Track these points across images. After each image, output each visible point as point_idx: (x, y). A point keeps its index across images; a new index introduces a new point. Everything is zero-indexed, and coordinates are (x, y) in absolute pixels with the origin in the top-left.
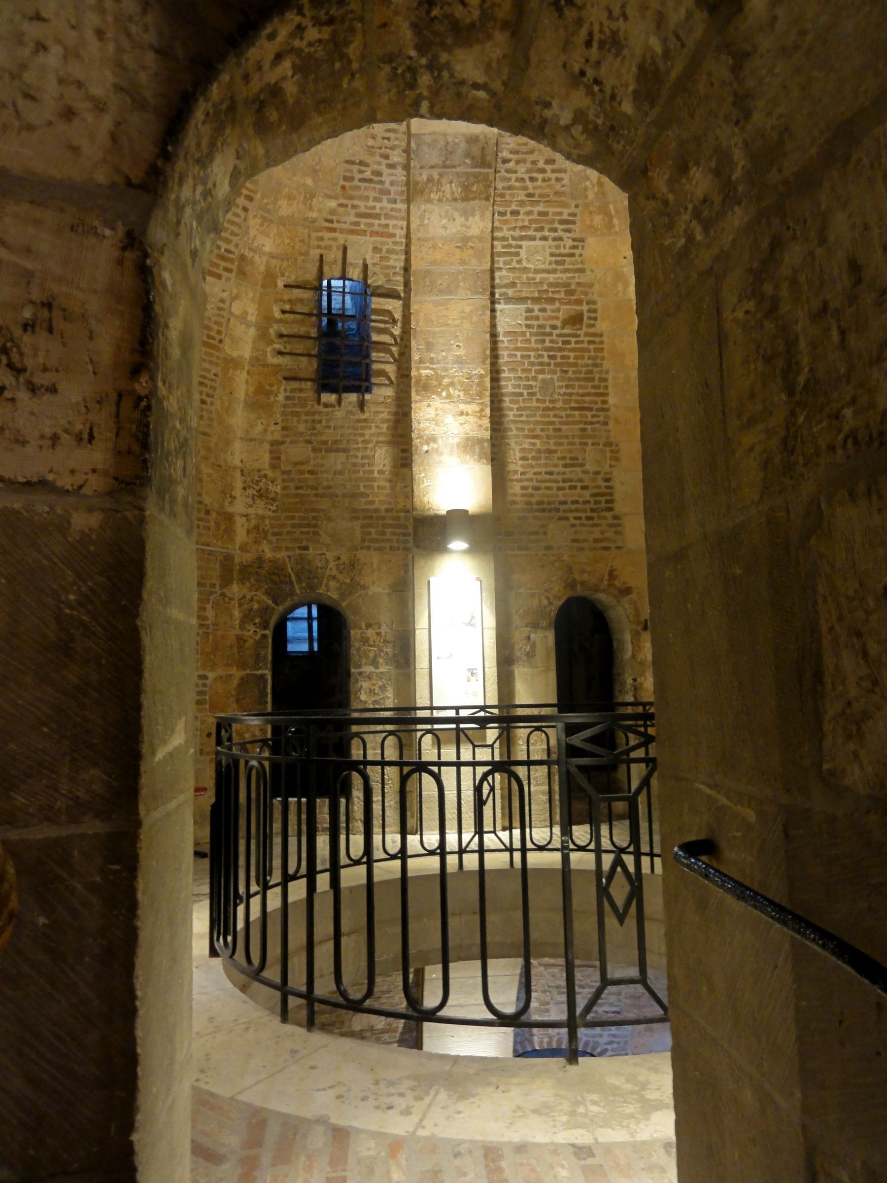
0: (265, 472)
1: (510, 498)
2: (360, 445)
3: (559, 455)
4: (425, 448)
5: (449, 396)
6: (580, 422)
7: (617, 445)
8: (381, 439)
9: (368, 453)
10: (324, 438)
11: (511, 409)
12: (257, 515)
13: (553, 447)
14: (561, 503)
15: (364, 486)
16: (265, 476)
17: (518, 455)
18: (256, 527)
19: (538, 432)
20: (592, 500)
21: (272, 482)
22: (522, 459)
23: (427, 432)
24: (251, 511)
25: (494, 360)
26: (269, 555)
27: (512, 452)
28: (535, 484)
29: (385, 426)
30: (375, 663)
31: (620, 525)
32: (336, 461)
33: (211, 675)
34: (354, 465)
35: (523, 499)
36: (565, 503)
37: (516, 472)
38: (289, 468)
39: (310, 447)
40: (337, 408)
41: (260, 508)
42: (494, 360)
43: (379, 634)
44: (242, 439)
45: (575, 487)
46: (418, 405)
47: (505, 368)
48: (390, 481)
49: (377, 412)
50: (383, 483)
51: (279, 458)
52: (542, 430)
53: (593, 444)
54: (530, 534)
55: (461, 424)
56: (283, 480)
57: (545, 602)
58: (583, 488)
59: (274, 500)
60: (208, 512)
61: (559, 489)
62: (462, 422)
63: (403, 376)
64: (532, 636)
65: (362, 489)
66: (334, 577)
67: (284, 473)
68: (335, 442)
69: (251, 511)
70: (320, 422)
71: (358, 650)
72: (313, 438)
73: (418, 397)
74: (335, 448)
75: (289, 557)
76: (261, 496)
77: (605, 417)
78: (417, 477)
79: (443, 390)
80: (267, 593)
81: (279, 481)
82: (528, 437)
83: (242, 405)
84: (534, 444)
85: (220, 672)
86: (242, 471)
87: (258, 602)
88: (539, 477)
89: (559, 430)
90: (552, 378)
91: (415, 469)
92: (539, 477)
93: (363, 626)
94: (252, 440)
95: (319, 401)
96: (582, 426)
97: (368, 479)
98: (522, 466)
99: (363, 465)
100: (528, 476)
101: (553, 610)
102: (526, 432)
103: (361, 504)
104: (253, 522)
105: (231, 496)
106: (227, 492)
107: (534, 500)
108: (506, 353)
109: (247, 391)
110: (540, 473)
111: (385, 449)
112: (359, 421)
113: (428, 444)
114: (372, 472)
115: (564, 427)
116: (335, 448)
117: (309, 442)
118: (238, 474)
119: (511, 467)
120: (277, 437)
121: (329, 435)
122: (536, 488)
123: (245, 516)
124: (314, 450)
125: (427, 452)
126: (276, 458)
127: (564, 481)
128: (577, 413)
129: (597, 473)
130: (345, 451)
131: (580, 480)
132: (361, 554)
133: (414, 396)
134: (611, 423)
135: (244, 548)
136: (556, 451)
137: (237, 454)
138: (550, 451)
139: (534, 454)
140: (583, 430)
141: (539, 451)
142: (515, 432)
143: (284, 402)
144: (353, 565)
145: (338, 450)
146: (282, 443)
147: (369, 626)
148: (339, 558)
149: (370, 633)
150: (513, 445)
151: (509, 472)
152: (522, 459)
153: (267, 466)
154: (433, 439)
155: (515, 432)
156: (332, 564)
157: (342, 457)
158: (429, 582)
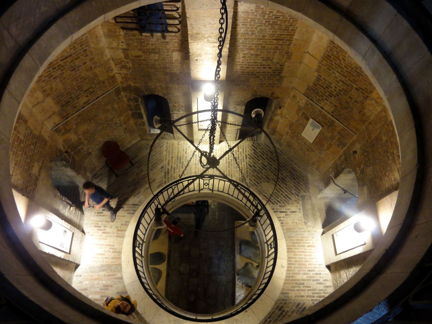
0: (123, 60)
1: (235, 70)
2: (165, 51)
3: (261, 56)
4: (196, 58)
5: (208, 41)
6: (276, 44)
7: (291, 54)
8: (175, 49)
9: (169, 53)
10: (147, 48)
11: (242, 39)
12: (124, 73)
13: (259, 53)
14: (257, 72)
15: (169, 65)
16: (124, 61)
17: (241, 55)
18: (125, 77)
19: (254, 47)
20: (272, 72)
21: (127, 63)
22: (243, 57)
23: (197, 53)
24: (121, 72)
25: (235, 21)
26: (132, 84)
27: (238, 55)
28: (247, 66)
29: (176, 45)
30: (178, 111)
31: (282, 80)
32: (155, 57)
33: (122, 118)
34: (163, 58)
35: (241, 71)
36: (260, 72)
37: (239, 62)
38: (133, 58)
39: (141, 51)
40: (152, 38)
41: (124, 71)
42: (235, 21)
43: (179, 105)
44: (107, 48)
45: (266, 68)
46: (193, 44)
47: (240, 24)
48: (181, 64)
49: (172, 39)
50: (177, 64)
51: (128, 55)
52: (255, 47)
53: (279, 53)
54: (241, 81)
55: (214, 50)
56: (132, 63)
57: (243, 99)
58: (269, 68)
59: (130, 69)
60: (104, 82)
61: (258, 68)
62: (214, 49)
63: (184, 26)
64: (237, 107)
65: (168, 66)
66: (160, 91)
67: (131, 60)
68: (153, 49)
69: (121, 72)
70: (144, 42)
71: (172, 108)
72: (142, 48)
73: (192, 41)
74: (154, 51)
75: (141, 85)
76: (124, 67)
77: (289, 43)
78: (192, 68)
79: (205, 39)
80: (135, 94)
81: (130, 62)
82: (248, 49)
83: (103, 36)
84: (250, 52)
85: (125, 115)
86: (112, 59)
87: (132, 96)
88: (250, 64)
89: (264, 47)
90: (266, 29)
91: (191, 65)
92: (250, 64)
93: (173, 103)
94: (113, 48)
95: (142, 35)
96: (277, 46)
97: (170, 63)
98: (243, 60)
99: (168, 58)
100: (245, 63)
101: (246, 101)
102: (247, 47)
103: (168, 71)
104: (123, 76)
105: (111, 70)
106: (110, 70)
107: (245, 71)
108: (242, 19)
109: (104, 32)
110: (250, 62)
111: (177, 53)
112: (163, 42)
113: (197, 57)
114: (172, 60)
115: (267, 46)
116: (154, 51)
117: (140, 49)
118: (111, 60)
119: (237, 60)
120: (125, 47)
121: (150, 47)
122: (248, 68)
123: (119, 73)
124: (143, 52)
125: (197, 60)
126: (127, 56)
127: (261, 65)
128: (275, 41)
129: (277, 63)
130: (158, 53)
131: (269, 65)
132: (170, 85)
133: (190, 41)
134: (292, 46)
135: (122, 83)
136: (260, 55)
137: (108, 54)
138: (257, 55)
139: (249, 55)
140: (276, 47)
141: (252, 55)
142: (241, 47)
143: (124, 35)
144: (167, 88)
145: (155, 53)
146: (128, 50)
147: (175, 103)
148: (161, 86)
149: (176, 104)
150: (240, 52)
151: (236, 62)
152: (243, 57)
153: (123, 57)
154: (200, 55)
155: (241, 47)
156: (158, 88)
157: (158, 55)
158: (197, 98)
